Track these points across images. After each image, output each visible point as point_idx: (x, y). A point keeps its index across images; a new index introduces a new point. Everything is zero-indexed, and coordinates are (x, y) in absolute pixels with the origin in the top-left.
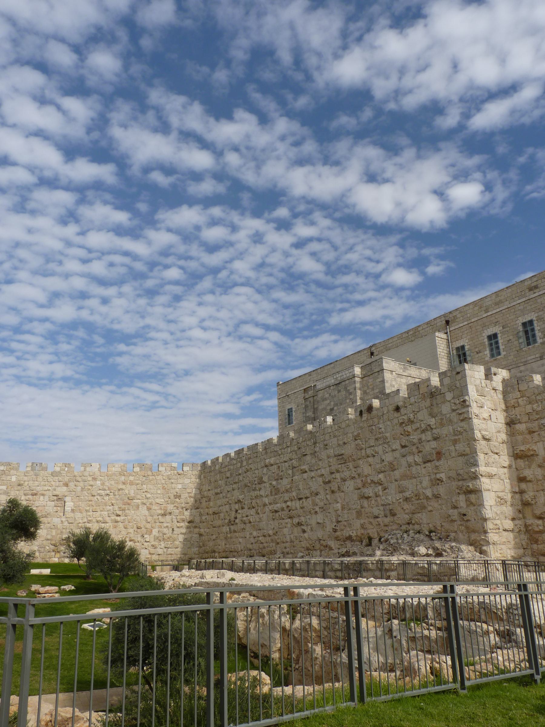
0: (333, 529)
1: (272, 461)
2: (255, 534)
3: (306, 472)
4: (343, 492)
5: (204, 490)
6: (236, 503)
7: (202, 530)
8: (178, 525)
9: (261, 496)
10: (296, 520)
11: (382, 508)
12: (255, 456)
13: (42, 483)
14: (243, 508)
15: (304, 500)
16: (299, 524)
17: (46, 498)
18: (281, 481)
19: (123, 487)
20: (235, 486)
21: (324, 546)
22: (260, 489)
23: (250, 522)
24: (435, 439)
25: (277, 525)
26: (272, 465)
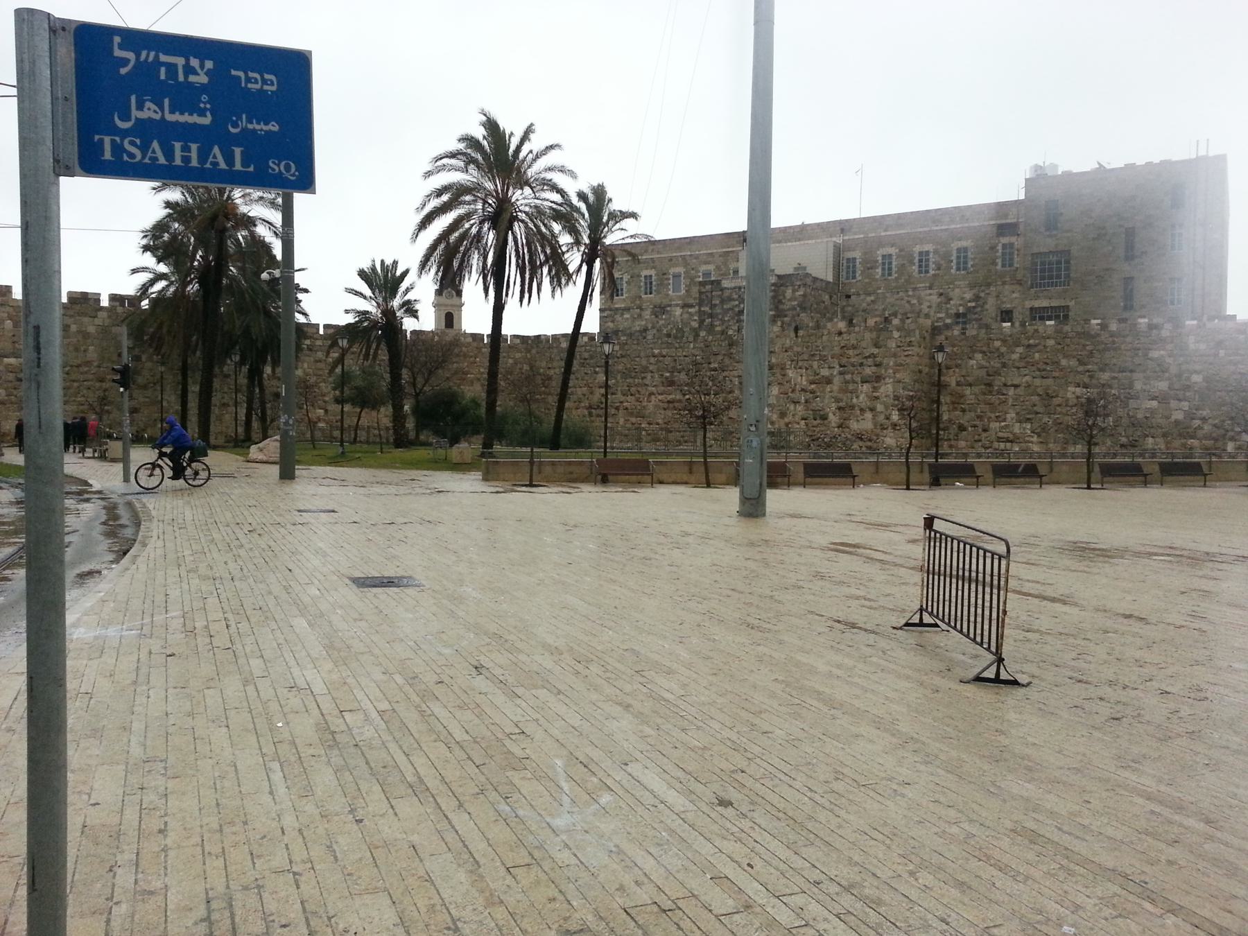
2: (633, 420)
11: (811, 412)
24: (876, 365)
25: (670, 415)
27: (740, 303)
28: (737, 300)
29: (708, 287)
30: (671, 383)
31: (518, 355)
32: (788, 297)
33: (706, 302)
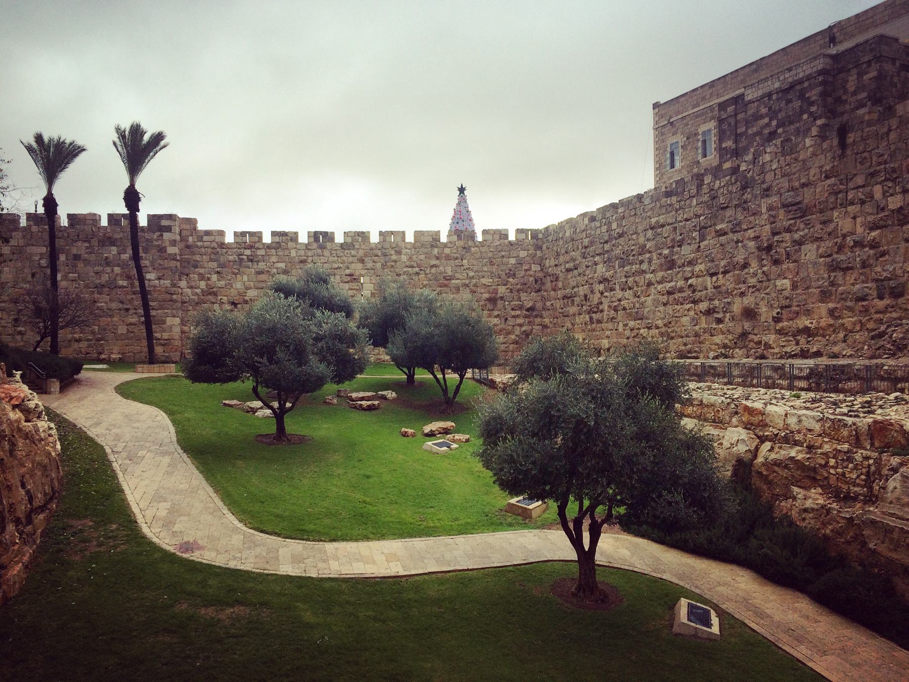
0: (774, 318)
1: (662, 219)
2: (632, 324)
3: (725, 234)
4: (795, 261)
5: (547, 265)
6: (600, 282)
7: (547, 320)
8: (513, 313)
9: (644, 272)
10: (703, 306)
12: (633, 213)
13: (331, 259)
14: (612, 290)
15: (720, 276)
16: (709, 312)
17: (338, 277)
18: (679, 249)
19: (437, 262)
20: (597, 259)
21: (756, 343)
22: (642, 262)
23: (624, 309)
26: (663, 226)
27: (771, 120)
28: (767, 115)
29: (731, 109)
30: (671, 264)
31: (523, 254)
32: (852, 89)
33: (728, 133)
